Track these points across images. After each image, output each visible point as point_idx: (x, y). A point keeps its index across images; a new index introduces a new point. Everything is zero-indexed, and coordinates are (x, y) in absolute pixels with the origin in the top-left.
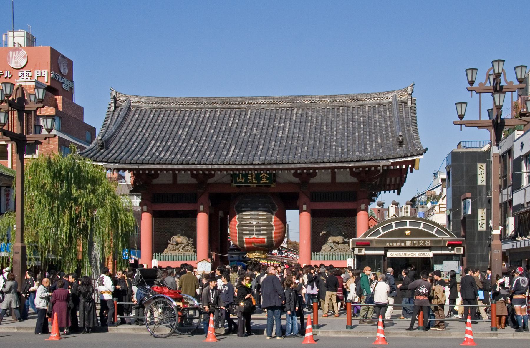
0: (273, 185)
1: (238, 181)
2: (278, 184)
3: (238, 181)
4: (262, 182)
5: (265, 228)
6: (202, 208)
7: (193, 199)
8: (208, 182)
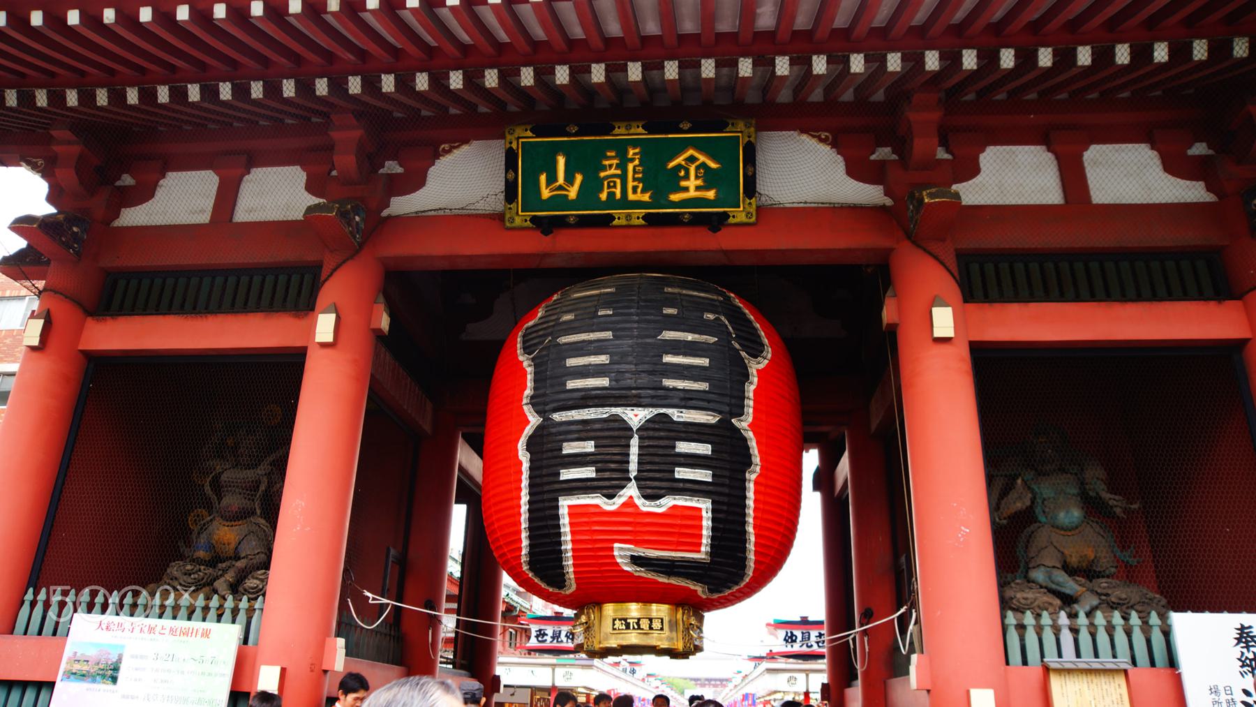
0: (739, 215)
1: (546, 193)
2: (766, 213)
4: (675, 197)
5: (704, 449)
6: (325, 326)
7: (295, 291)
8: (385, 213)
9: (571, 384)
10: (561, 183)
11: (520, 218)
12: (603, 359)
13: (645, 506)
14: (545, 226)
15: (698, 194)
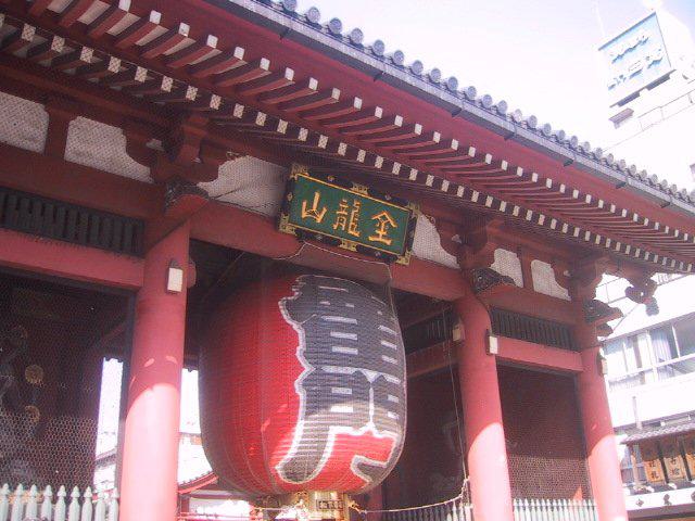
1: (304, 215)
2: (414, 259)
3: (304, 215)
6: (176, 280)
9: (335, 349)
10: (312, 210)
11: (288, 228)
12: (353, 336)
13: (377, 435)
14: (301, 236)
15: (383, 240)
